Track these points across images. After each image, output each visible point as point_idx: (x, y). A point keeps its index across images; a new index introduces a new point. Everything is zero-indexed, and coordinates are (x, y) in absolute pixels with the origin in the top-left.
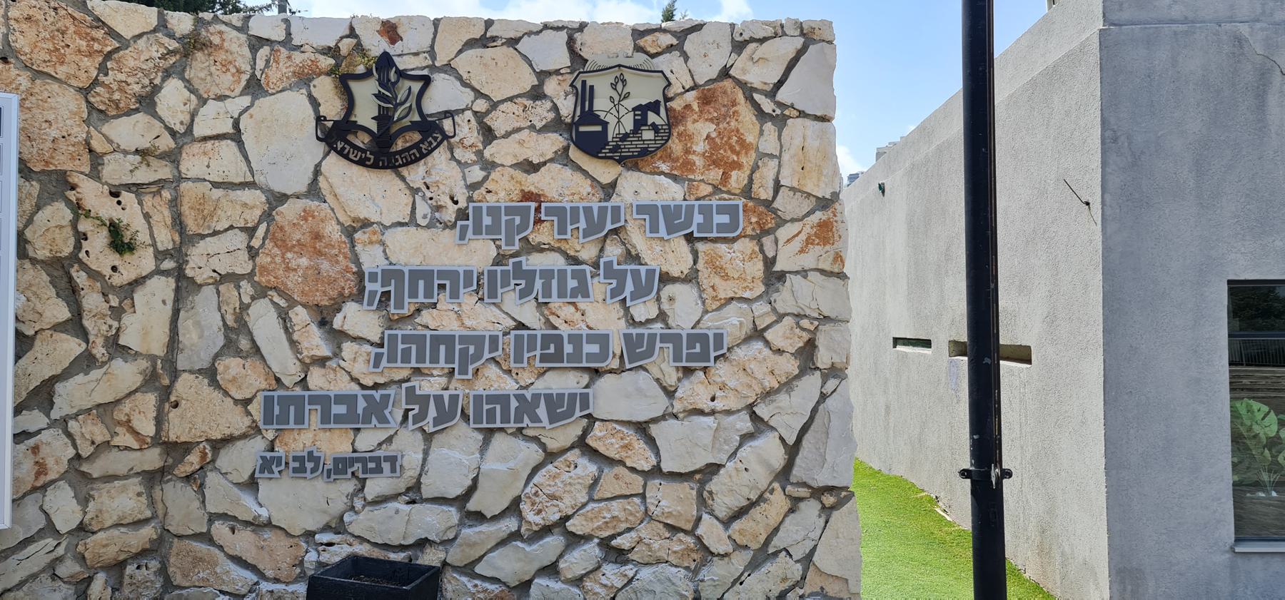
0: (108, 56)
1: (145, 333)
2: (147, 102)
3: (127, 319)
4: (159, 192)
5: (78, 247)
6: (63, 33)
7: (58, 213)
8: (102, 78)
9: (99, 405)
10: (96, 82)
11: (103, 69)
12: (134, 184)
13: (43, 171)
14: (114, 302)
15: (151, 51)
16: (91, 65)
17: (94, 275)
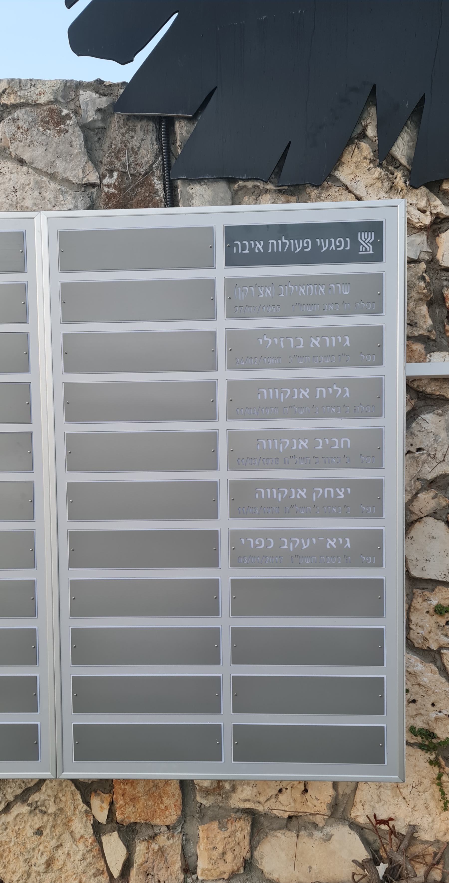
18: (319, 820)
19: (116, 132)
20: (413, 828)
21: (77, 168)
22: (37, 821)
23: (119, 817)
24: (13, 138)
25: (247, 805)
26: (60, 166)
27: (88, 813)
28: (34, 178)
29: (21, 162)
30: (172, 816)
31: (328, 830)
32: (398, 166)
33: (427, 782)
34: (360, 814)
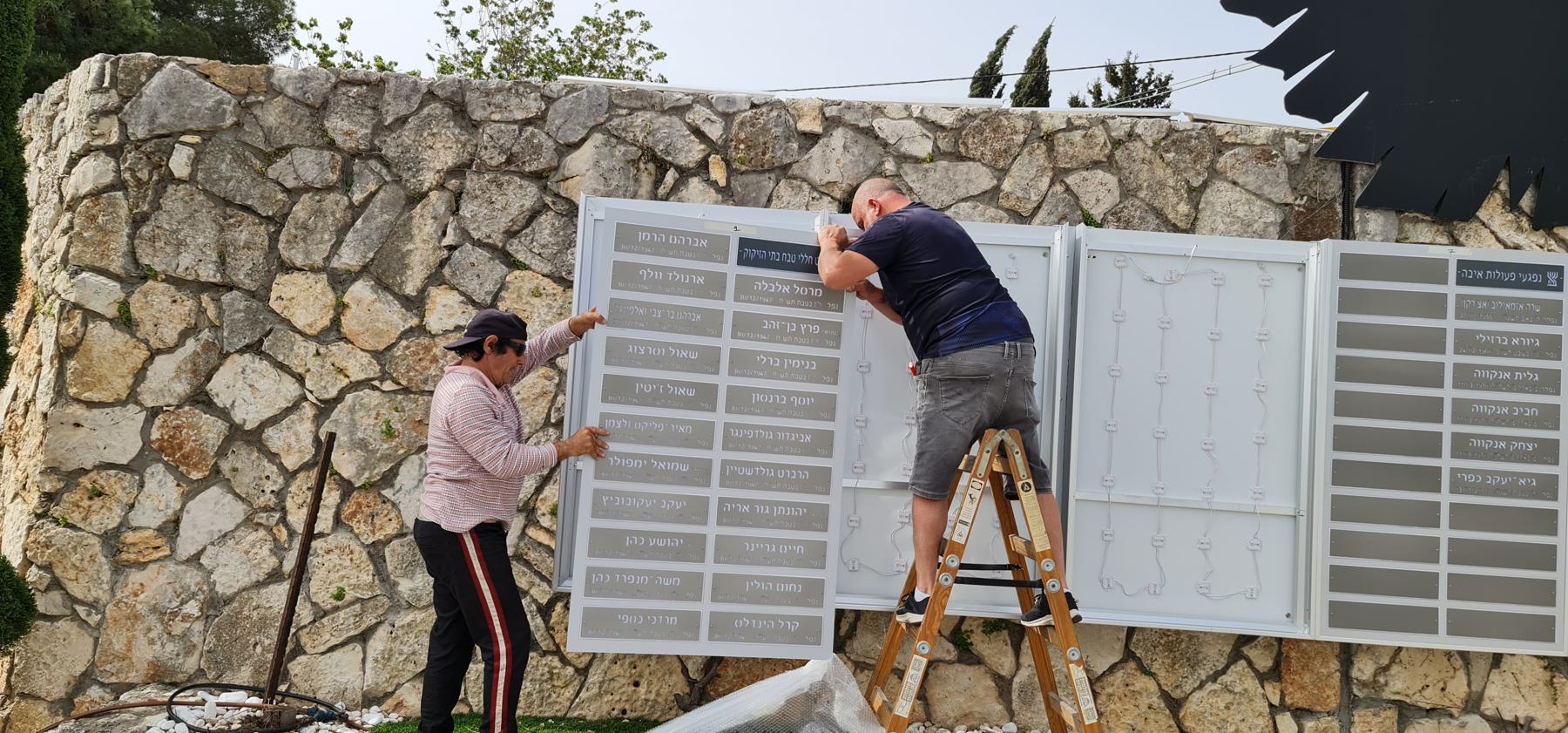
18: (1455, 711)
19: (1311, 169)
20: (1531, 720)
21: (1283, 194)
22: (1229, 698)
23: (1288, 701)
24: (1233, 167)
25: (1397, 697)
26: (1267, 190)
27: (1264, 696)
28: (1245, 196)
29: (1235, 183)
30: (1333, 703)
31: (1464, 718)
32: (1522, 212)
33: (1541, 684)
34: (1488, 707)
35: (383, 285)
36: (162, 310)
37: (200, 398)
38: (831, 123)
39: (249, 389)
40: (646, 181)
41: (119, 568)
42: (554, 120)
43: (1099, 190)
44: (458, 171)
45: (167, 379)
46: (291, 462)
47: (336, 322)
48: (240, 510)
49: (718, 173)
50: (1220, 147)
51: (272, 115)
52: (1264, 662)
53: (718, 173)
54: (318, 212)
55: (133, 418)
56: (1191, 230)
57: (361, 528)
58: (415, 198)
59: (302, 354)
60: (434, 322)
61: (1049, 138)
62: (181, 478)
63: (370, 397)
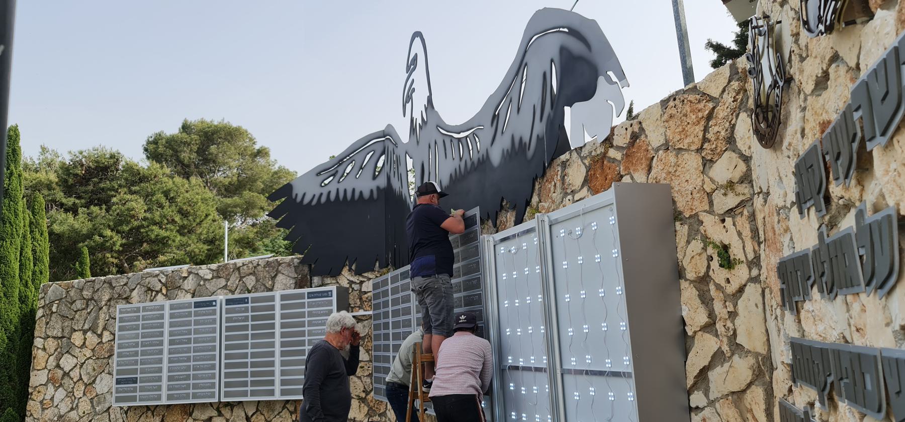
0: (710, 117)
1: (749, 334)
2: (731, 140)
3: (738, 321)
4: (742, 214)
5: (709, 267)
6: (686, 115)
7: (696, 245)
8: (708, 136)
9: (733, 393)
10: (705, 140)
11: (706, 130)
12: (731, 210)
13: (691, 217)
14: (731, 309)
15: (728, 98)
16: (699, 129)
17: (719, 287)
19: (301, 268)
35: (94, 332)
36: (51, 344)
37: (58, 366)
38: (190, 273)
39: (67, 362)
40: (149, 296)
41: (43, 409)
42: (129, 284)
43: (250, 281)
44: (109, 300)
45: (52, 362)
46: (75, 380)
47: (84, 343)
48: (65, 393)
49: (164, 291)
50: (280, 264)
51: (72, 293)
52: (292, 409)
53: (164, 291)
54: (80, 316)
55: (46, 371)
56: (271, 290)
57: (88, 395)
58: (101, 308)
59: (78, 350)
60: (104, 341)
61: (239, 269)
62: (55, 386)
63: (90, 361)
